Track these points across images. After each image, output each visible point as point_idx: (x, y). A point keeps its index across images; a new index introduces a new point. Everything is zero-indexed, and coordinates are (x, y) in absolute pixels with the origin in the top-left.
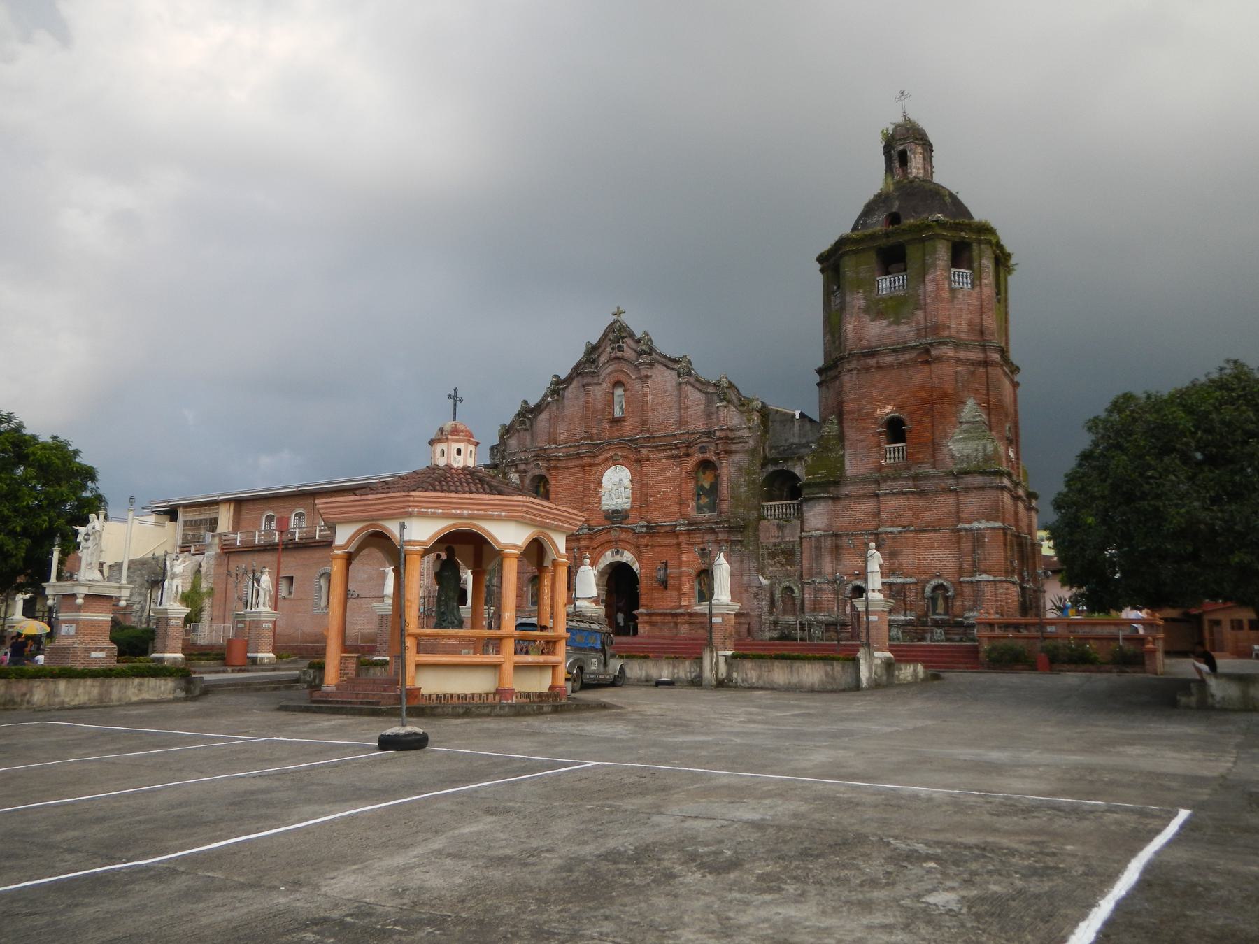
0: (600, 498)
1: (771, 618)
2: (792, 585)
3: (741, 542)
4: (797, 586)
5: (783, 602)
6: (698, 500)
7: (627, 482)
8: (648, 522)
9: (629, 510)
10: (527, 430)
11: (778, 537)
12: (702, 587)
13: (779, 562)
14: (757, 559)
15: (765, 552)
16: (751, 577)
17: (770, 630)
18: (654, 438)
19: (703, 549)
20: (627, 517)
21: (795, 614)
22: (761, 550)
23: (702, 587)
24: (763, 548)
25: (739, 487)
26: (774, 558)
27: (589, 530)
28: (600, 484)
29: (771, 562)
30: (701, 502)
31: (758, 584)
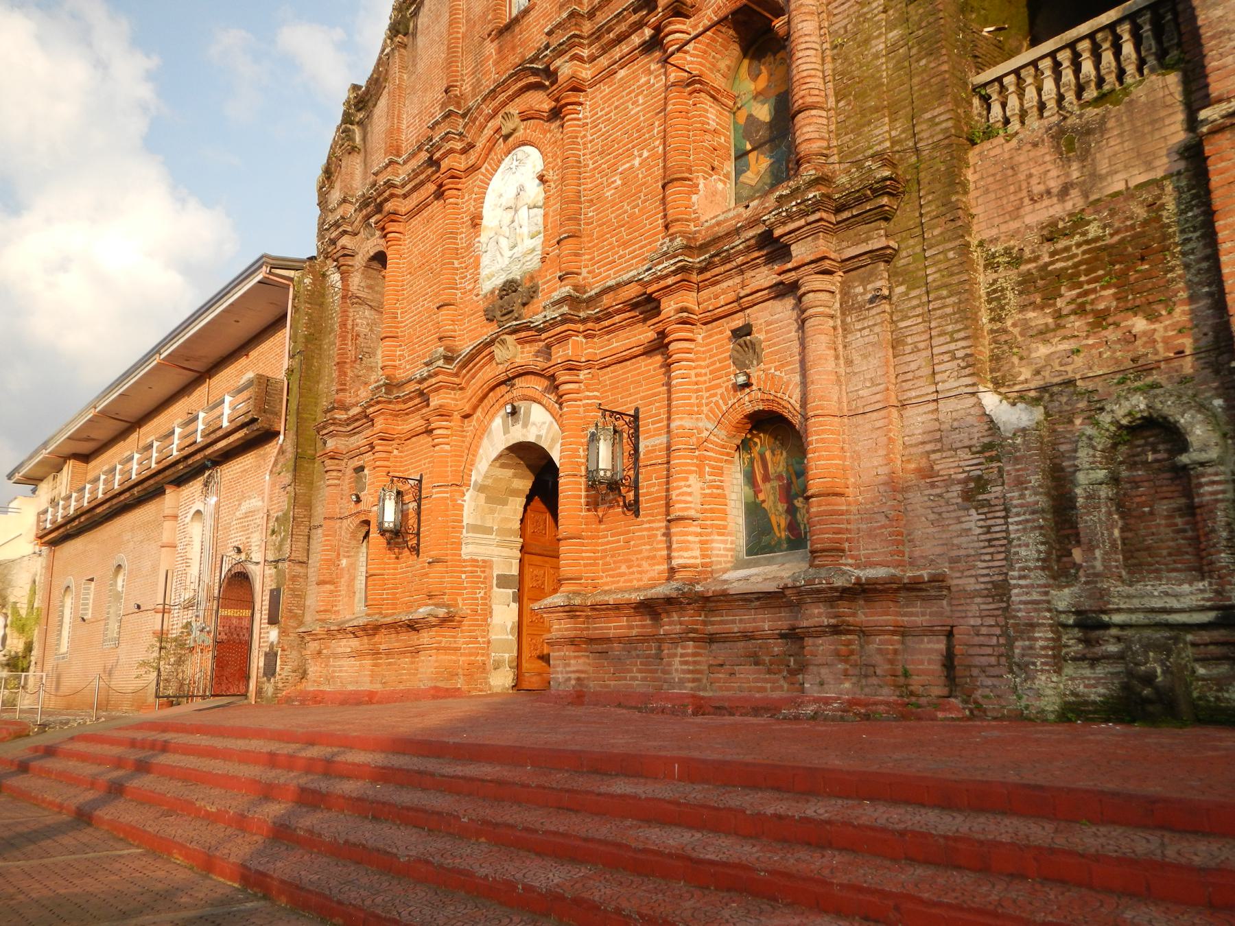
0: (477, 265)
1: (1064, 598)
2: (1168, 408)
3: (885, 256)
4: (1201, 408)
5: (1121, 505)
6: (739, 173)
7: (535, 192)
8: (576, 288)
9: (540, 270)
10: (353, 150)
11: (1064, 192)
12: (756, 494)
13: (1081, 311)
14: (966, 315)
15: (1007, 277)
16: (945, 406)
17: (1058, 661)
18: (591, 15)
19: (742, 332)
20: (533, 292)
21: (1202, 568)
22: (983, 279)
23: (756, 494)
24: (991, 264)
25: (867, 41)
26: (1050, 296)
27: (448, 360)
28: (476, 222)
29: (1038, 318)
30: (750, 177)
31: (978, 435)
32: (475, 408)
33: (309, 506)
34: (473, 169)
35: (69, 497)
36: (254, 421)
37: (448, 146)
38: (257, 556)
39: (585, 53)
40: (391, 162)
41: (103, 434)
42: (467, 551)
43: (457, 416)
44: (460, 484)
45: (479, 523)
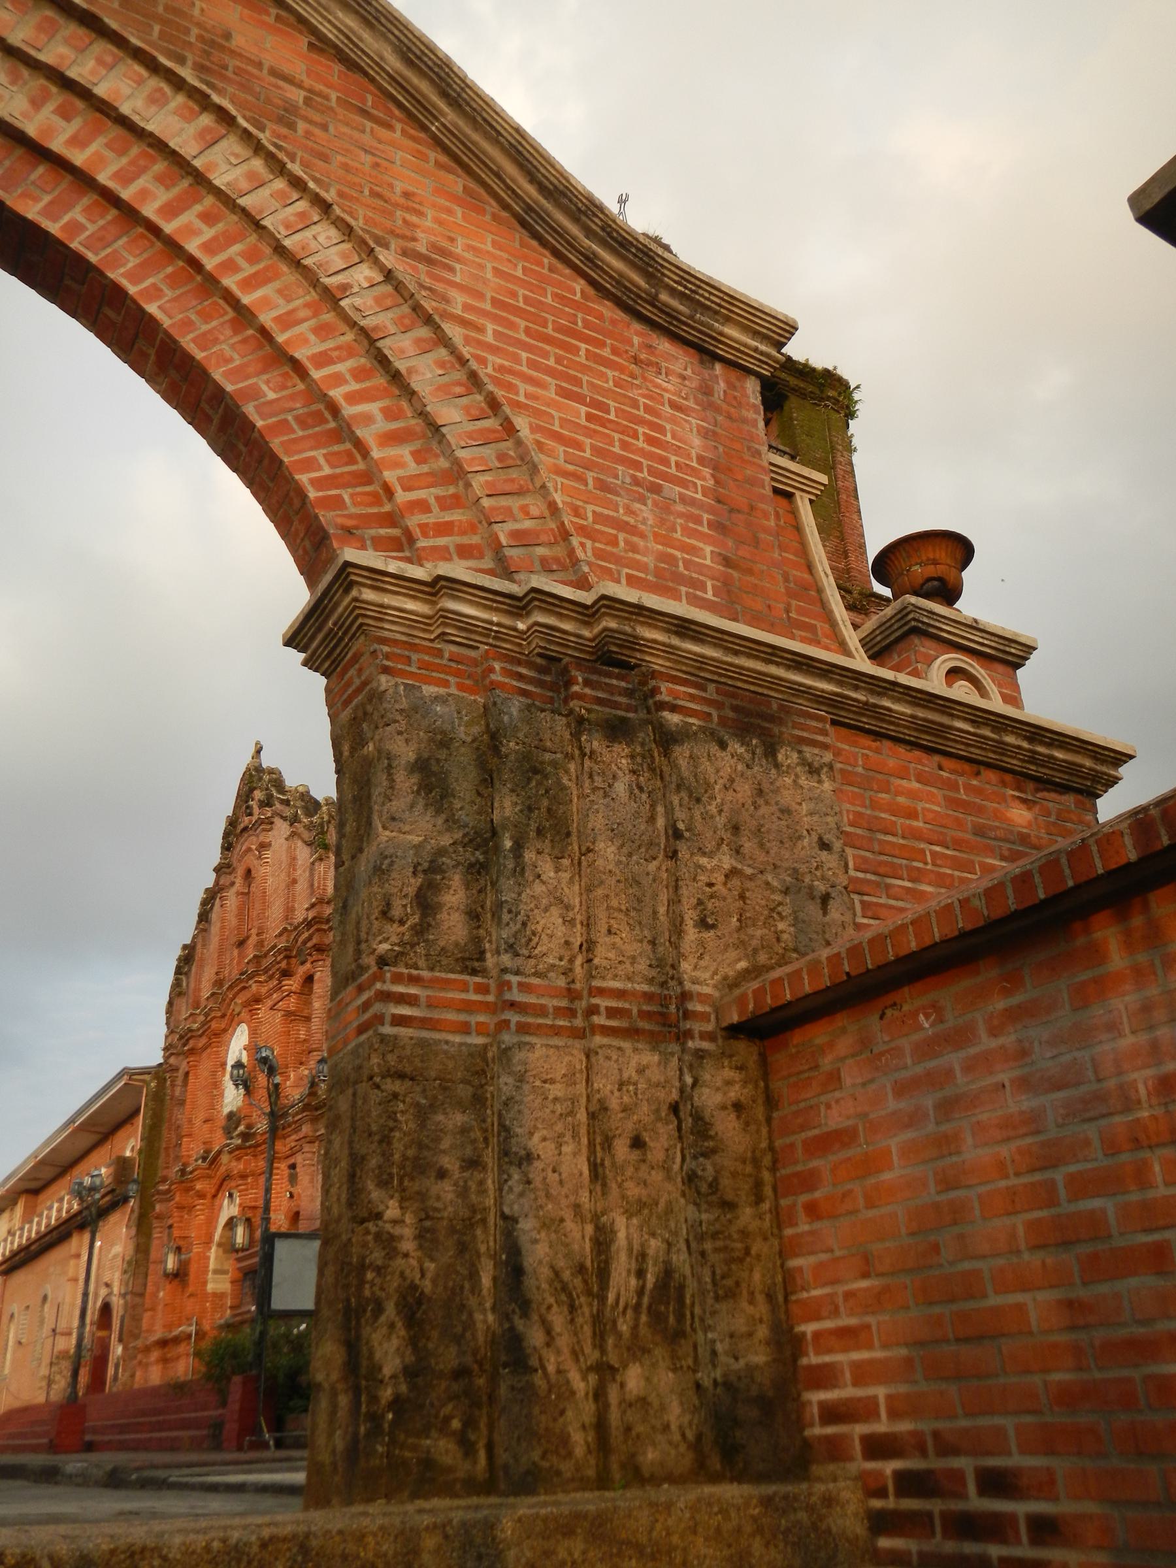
10: (180, 994)
19: (293, 1166)
27: (204, 1159)
32: (218, 1191)
33: (146, 1252)
34: (225, 1030)
35: (22, 1229)
36: (113, 1191)
37: (213, 1015)
38: (116, 1290)
39: (262, 978)
40: (192, 1014)
41: (48, 1173)
42: (210, 1287)
43: (209, 1196)
44: (208, 1242)
45: (219, 1267)
